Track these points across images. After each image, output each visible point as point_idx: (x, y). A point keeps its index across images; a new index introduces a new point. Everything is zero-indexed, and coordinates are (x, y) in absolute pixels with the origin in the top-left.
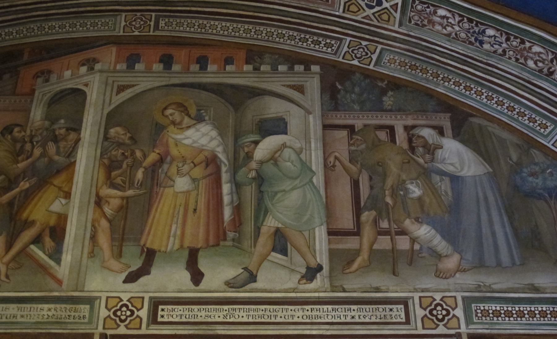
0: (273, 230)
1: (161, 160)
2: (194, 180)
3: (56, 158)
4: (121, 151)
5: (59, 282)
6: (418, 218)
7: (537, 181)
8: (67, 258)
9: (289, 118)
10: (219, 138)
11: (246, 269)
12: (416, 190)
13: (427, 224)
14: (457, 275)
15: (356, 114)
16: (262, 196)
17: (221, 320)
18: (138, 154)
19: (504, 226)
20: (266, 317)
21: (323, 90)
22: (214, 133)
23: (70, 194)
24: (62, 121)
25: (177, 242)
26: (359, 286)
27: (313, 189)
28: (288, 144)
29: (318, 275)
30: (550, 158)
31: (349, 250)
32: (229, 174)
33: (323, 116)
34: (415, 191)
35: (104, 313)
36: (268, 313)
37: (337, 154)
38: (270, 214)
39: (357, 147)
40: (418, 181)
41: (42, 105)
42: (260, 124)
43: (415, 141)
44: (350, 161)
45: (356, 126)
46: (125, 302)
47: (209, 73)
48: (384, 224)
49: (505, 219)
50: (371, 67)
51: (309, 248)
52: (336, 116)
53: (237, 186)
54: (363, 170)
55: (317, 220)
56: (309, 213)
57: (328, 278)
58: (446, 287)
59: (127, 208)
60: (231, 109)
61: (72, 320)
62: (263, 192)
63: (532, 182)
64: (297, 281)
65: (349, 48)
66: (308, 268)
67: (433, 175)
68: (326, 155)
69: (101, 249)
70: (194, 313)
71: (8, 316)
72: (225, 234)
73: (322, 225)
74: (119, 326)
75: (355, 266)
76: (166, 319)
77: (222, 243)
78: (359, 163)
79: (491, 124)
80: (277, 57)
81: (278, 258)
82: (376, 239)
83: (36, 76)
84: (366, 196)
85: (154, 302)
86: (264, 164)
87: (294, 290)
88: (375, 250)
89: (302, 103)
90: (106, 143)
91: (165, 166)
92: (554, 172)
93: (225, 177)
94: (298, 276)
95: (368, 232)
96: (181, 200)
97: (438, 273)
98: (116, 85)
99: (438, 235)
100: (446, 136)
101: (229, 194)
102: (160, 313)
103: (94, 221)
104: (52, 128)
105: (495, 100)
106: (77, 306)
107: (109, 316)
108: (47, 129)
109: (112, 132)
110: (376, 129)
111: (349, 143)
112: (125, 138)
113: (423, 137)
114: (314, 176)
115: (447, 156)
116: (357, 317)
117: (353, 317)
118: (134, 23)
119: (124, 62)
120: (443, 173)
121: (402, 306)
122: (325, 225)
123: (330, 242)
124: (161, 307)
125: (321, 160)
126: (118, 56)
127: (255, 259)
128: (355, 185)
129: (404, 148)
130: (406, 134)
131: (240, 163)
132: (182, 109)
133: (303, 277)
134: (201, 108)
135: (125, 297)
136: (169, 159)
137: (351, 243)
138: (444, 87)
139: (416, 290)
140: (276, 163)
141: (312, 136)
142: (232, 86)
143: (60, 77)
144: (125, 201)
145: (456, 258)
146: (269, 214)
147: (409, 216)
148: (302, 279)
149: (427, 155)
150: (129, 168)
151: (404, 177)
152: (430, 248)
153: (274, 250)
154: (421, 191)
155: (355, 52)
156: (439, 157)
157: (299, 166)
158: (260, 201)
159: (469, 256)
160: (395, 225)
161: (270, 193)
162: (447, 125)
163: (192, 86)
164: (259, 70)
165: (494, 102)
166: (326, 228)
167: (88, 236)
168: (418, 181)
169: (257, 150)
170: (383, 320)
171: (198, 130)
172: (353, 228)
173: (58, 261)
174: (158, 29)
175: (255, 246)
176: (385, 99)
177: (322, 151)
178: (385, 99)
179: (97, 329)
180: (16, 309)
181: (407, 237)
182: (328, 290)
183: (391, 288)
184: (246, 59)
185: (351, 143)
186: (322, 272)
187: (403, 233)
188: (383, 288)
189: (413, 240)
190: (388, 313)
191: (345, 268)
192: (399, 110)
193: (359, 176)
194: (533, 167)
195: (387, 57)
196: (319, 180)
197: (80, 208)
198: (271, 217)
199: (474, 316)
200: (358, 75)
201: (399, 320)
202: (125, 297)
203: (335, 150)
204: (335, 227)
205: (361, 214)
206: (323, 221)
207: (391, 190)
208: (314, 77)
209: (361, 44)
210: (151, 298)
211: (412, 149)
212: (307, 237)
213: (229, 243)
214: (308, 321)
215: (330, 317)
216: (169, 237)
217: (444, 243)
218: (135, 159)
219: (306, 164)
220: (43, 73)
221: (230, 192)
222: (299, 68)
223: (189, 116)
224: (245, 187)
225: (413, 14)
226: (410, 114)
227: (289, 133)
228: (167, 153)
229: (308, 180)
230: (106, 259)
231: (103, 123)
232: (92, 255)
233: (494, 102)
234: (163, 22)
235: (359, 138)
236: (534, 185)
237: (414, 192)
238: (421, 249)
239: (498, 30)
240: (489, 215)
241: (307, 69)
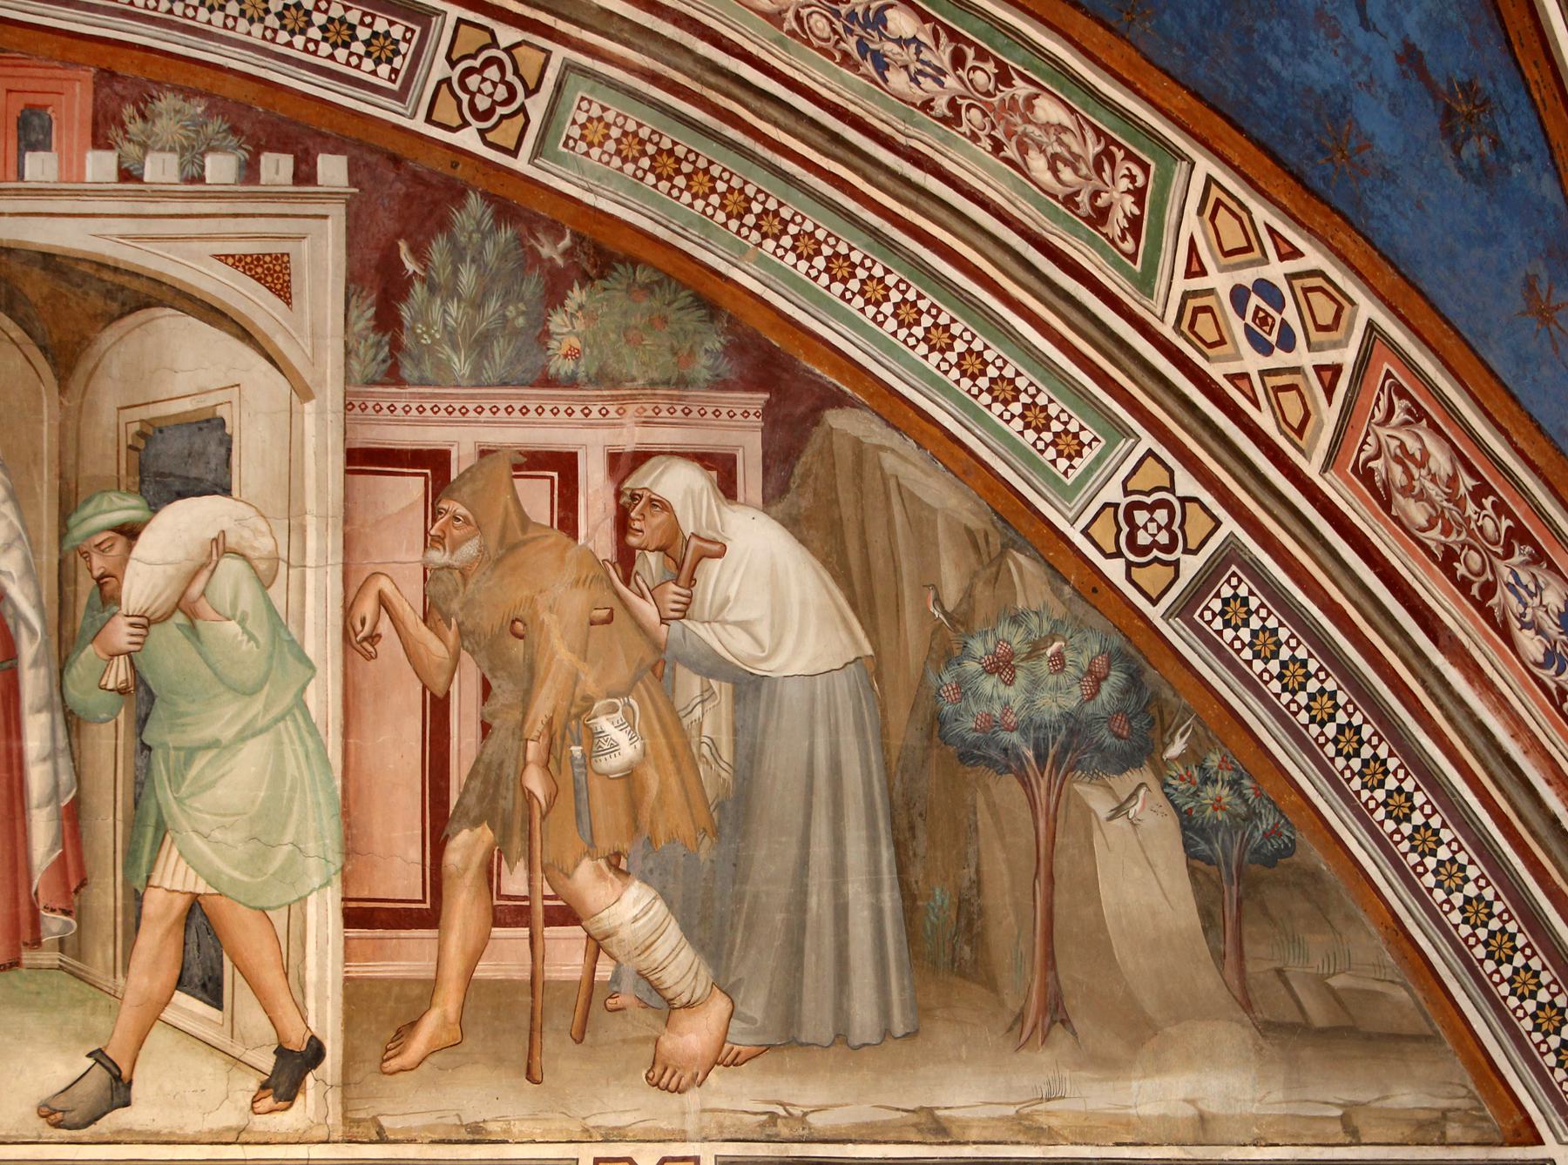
0: (180, 903)
6: (618, 855)
7: (1010, 692)
9: (236, 415)
11: (98, 1056)
12: (622, 737)
13: (644, 881)
15: (457, 396)
16: (148, 768)
19: (876, 887)
21: (354, 279)
26: (430, 1119)
27: (306, 735)
28: (232, 541)
29: (310, 1079)
30: (1067, 589)
31: (404, 982)
32: (43, 671)
33: (348, 407)
37: (384, 584)
38: (172, 842)
39: (452, 552)
40: (632, 701)
42: (141, 444)
43: (637, 525)
44: (425, 621)
45: (454, 456)
48: (514, 882)
49: (886, 854)
50: (521, 164)
51: (287, 975)
52: (392, 409)
53: (72, 722)
54: (465, 656)
56: (289, 836)
57: (339, 1090)
58: (676, 1124)
62: (150, 749)
63: (991, 699)
64: (249, 1100)
65: (453, 64)
66: (282, 1052)
67: (682, 671)
68: (353, 591)
73: (327, 883)
75: (418, 1044)
77: (27, 957)
78: (453, 621)
79: (893, 439)
80: (199, 110)
81: (192, 1015)
82: (486, 938)
86: (153, 628)
88: (479, 981)
89: (281, 342)
92: (1069, 656)
94: (253, 1084)
95: (463, 907)
97: (658, 1070)
99: (674, 921)
100: (740, 498)
101: (44, 760)
105: (927, 321)
110: (517, 467)
111: (426, 532)
113: (665, 506)
114: (310, 679)
115: (732, 593)
120: (714, 667)
122: (337, 882)
123: (347, 958)
127: (128, 1017)
128: (437, 711)
129: (601, 557)
130: (610, 492)
131: (78, 625)
133: (264, 1086)
138: (762, 261)
139: (587, 1137)
140: (192, 631)
141: (311, 504)
142: (50, 261)
145: (720, 1005)
146: (168, 838)
147: (591, 851)
148: (263, 1094)
149: (672, 587)
151: (589, 683)
153: (180, 984)
154: (638, 744)
155: (473, 82)
156: (709, 597)
159: (755, 1005)
160: (545, 883)
161: (172, 752)
162: (748, 446)
164: (139, 180)
165: (918, 331)
166: (340, 896)
168: (632, 701)
169: (133, 568)
172: (420, 897)
175: (126, 967)
176: (557, 322)
177: (339, 568)
178: (557, 322)
181: (577, 931)
182: (335, 1137)
183: (517, 1128)
184: (95, 124)
185: (432, 532)
186: (320, 1067)
188: (494, 1127)
189: (597, 945)
191: (390, 1053)
192: (602, 378)
193: (451, 680)
194: (1005, 630)
195: (582, 106)
196: (324, 697)
198: (175, 853)
200: (474, 202)
203: (379, 568)
204: (365, 894)
205: (445, 843)
206: (332, 869)
207: (544, 741)
208: (325, 217)
211: (626, 558)
212: (282, 933)
213: (48, 957)
217: (687, 955)
219: (286, 627)
221: (48, 745)
222: (277, 168)
224: (94, 727)
226: (633, 397)
227: (235, 493)
229: (288, 699)
233: (918, 331)
235: (462, 510)
236: (997, 711)
237: (615, 746)
238: (616, 978)
240: (838, 842)
241: (304, 174)
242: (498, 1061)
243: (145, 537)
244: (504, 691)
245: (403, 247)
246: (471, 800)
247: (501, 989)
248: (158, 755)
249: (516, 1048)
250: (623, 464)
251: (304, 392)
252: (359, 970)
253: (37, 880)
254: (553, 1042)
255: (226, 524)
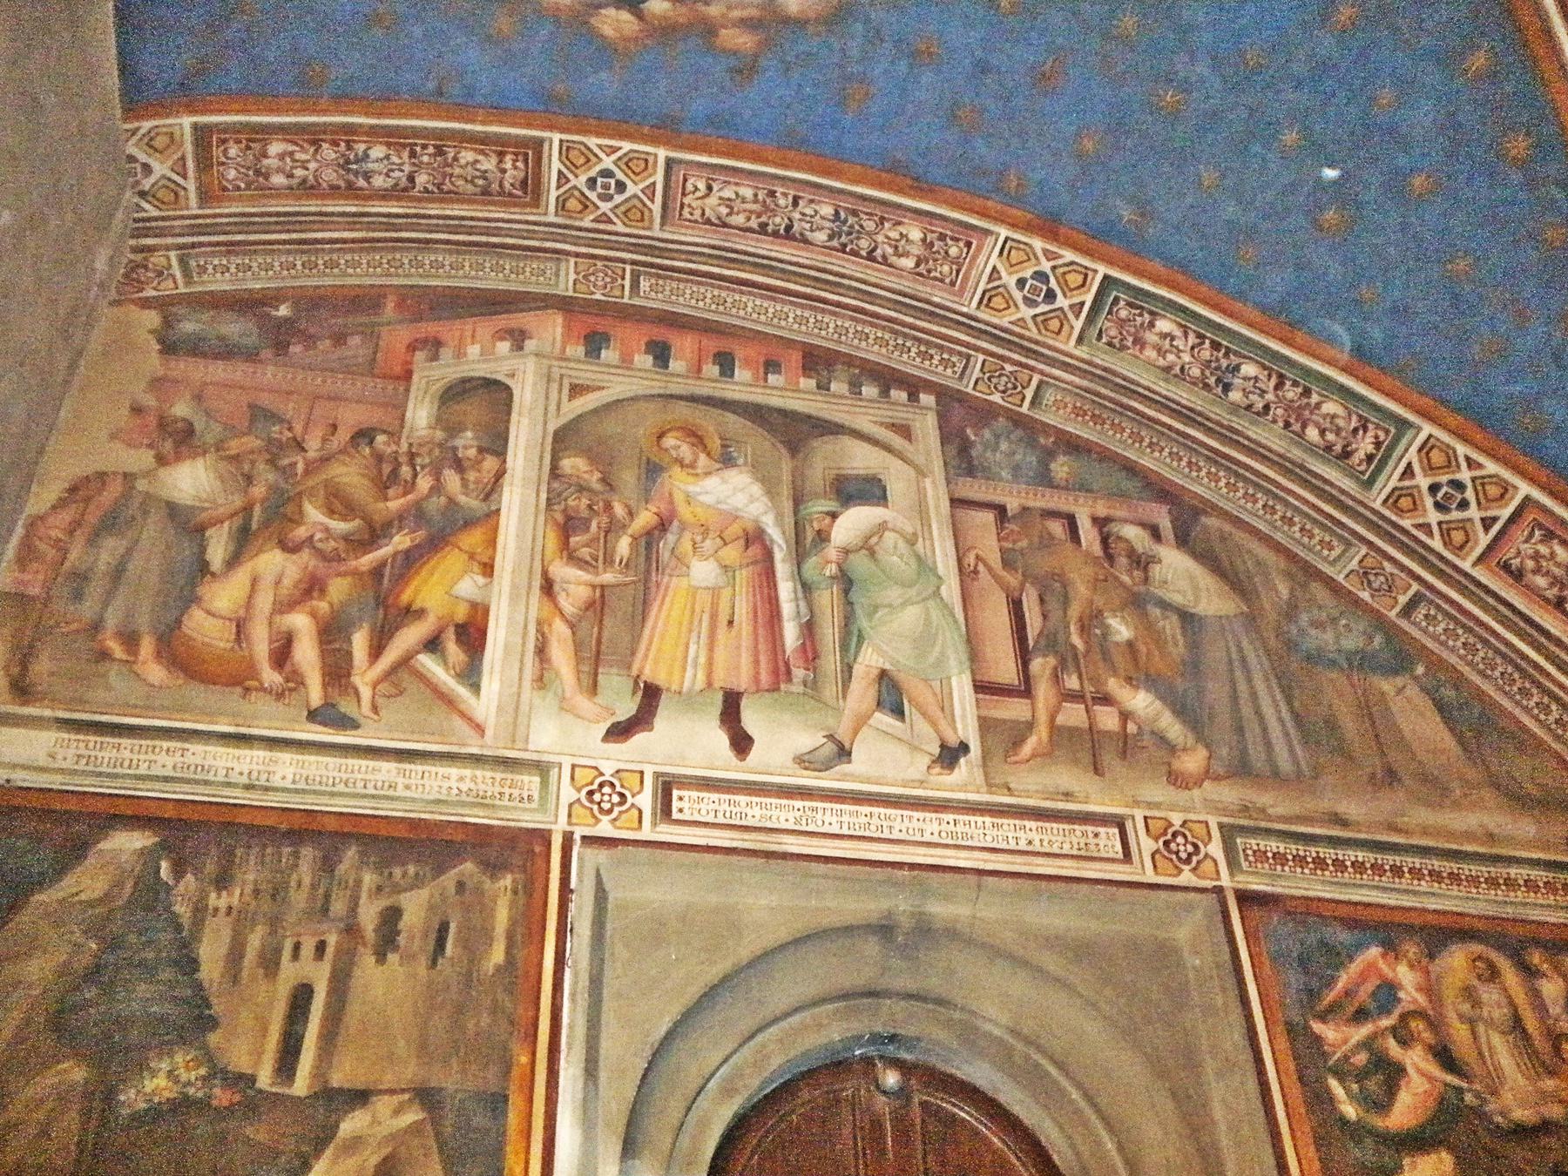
0: (876, 672)
1: (663, 525)
2: (725, 568)
3: (462, 499)
4: (585, 502)
5: (479, 729)
8: (491, 683)
10: (765, 499)
11: (831, 737)
14: (1206, 784)
17: (791, 826)
18: (619, 510)
20: (873, 828)
21: (945, 440)
22: (756, 489)
23: (492, 567)
24: (469, 434)
25: (701, 677)
29: (962, 760)
33: (948, 482)
34: (1121, 629)
35: (568, 794)
36: (875, 821)
37: (980, 553)
41: (427, 399)
45: (1008, 507)
46: (607, 778)
47: (736, 384)
48: (1072, 682)
53: (806, 588)
55: (953, 663)
56: (937, 649)
59: (603, 603)
60: (784, 451)
61: (506, 803)
66: (943, 746)
69: (557, 674)
70: (738, 809)
71: (380, 784)
72: (789, 672)
74: (598, 821)
75: (1027, 749)
76: (686, 816)
83: (412, 348)
84: (1037, 632)
85: (664, 783)
87: (921, 783)
90: (556, 485)
91: (671, 538)
93: (782, 568)
94: (927, 760)
96: (704, 599)
98: (566, 382)
102: (676, 804)
103: (539, 623)
104: (449, 444)
106: (518, 777)
107: (579, 800)
108: (440, 445)
109: (568, 464)
112: (594, 480)
113: (1127, 541)
116: (1037, 843)
117: (1030, 843)
118: (592, 278)
119: (577, 344)
120: (1165, 605)
121: (1116, 831)
122: (968, 673)
123: (978, 707)
124: (676, 793)
125: (953, 562)
126: (568, 328)
128: (1016, 608)
132: (693, 440)
133: (933, 762)
134: (728, 443)
135: (608, 769)
136: (676, 523)
137: (1014, 710)
139: (1137, 803)
141: (933, 515)
142: (783, 412)
143: (460, 354)
144: (598, 594)
145: (1202, 753)
147: (1115, 673)
150: (602, 534)
151: (1099, 601)
152: (1153, 732)
157: (913, 562)
158: (848, 619)
162: (1165, 524)
163: (709, 401)
164: (828, 390)
167: (531, 646)
170: (1083, 853)
171: (724, 481)
173: (476, 688)
174: (638, 295)
175: (844, 697)
176: (1053, 466)
179: (556, 822)
180: (394, 772)
187: (1106, 700)
189: (1125, 716)
190: (1092, 840)
195: (1049, 396)
197: (513, 599)
198: (870, 650)
199: (1242, 860)
201: (1111, 855)
202: (608, 769)
209: (1003, 368)
210: (657, 775)
211: (1110, 558)
212: (938, 690)
213: (797, 688)
214: (950, 842)
215: (989, 838)
216: (684, 669)
218: (612, 517)
220: (425, 341)
223: (708, 454)
225: (1109, 324)
228: (673, 514)
230: (568, 695)
231: (548, 448)
232: (540, 682)
234: (648, 284)
239: (1264, 367)
241: (913, 397)
242: (1076, 762)
243: (839, 521)
244: (1054, 605)
245: (968, 431)
246: (1043, 642)
247: (1073, 732)
248: (857, 607)
249: (1086, 758)
250: (1100, 522)
251: (921, 473)
252: (984, 713)
253: (788, 652)
254: (1109, 758)
255: (887, 518)
